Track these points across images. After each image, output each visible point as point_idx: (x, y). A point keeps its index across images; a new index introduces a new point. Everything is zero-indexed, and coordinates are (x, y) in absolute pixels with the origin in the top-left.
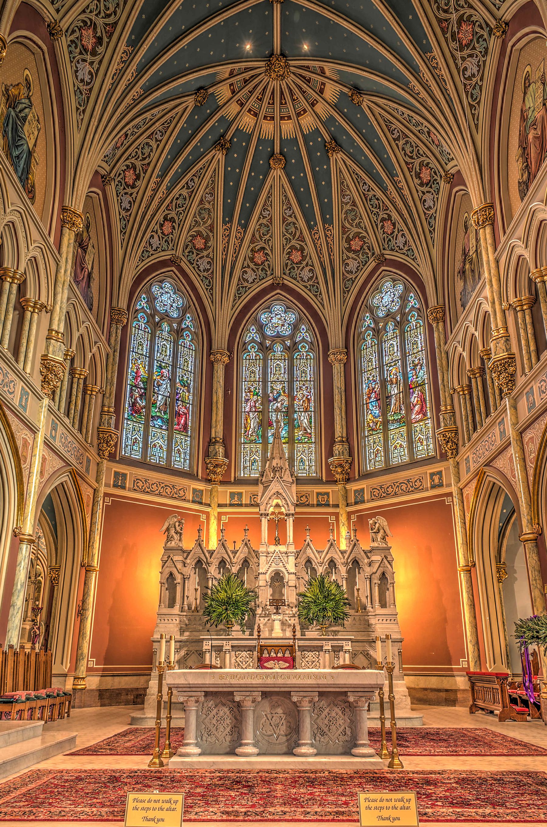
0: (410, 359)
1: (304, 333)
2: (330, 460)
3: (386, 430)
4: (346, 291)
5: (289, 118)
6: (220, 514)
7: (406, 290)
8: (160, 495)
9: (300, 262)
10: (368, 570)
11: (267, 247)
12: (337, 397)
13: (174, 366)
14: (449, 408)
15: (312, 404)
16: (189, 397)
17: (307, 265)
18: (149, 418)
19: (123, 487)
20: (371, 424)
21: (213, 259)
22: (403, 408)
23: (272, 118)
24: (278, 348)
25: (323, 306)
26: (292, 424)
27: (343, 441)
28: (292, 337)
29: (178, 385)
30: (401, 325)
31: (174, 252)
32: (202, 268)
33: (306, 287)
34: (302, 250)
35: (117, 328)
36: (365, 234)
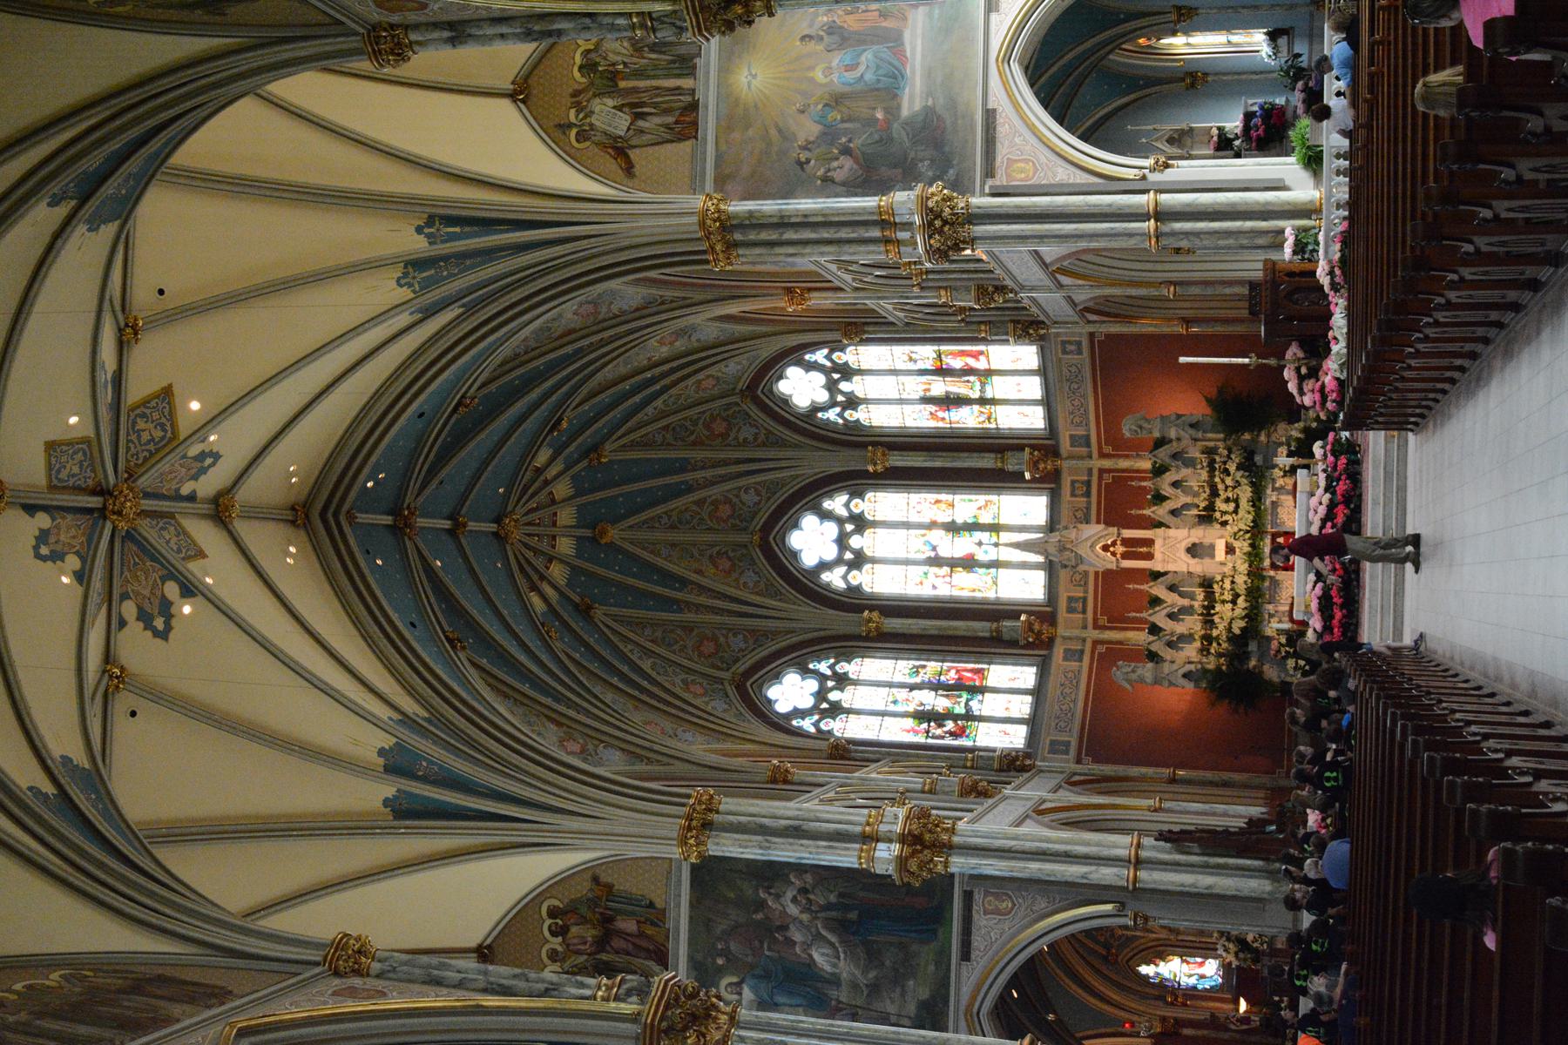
0: (900, 366)
1: (837, 504)
2: (1027, 476)
3: (993, 402)
4: (782, 444)
5: (555, 514)
6: (1096, 626)
7: (800, 363)
8: (1074, 701)
9: (733, 506)
10: (1186, 442)
11: (709, 552)
12: (938, 464)
13: (890, 685)
14: (983, 327)
15: (944, 497)
16: (932, 667)
17: (737, 496)
18: (969, 716)
19: (1068, 744)
20: (981, 419)
21: (730, 630)
22: (966, 378)
23: (554, 538)
24: (855, 542)
25: (797, 476)
26: (973, 527)
27: (1002, 458)
28: (840, 521)
29: (918, 680)
30: (847, 372)
31: (726, 684)
32: (742, 645)
33: (769, 498)
34: (715, 503)
35: (856, 751)
36: (708, 414)
